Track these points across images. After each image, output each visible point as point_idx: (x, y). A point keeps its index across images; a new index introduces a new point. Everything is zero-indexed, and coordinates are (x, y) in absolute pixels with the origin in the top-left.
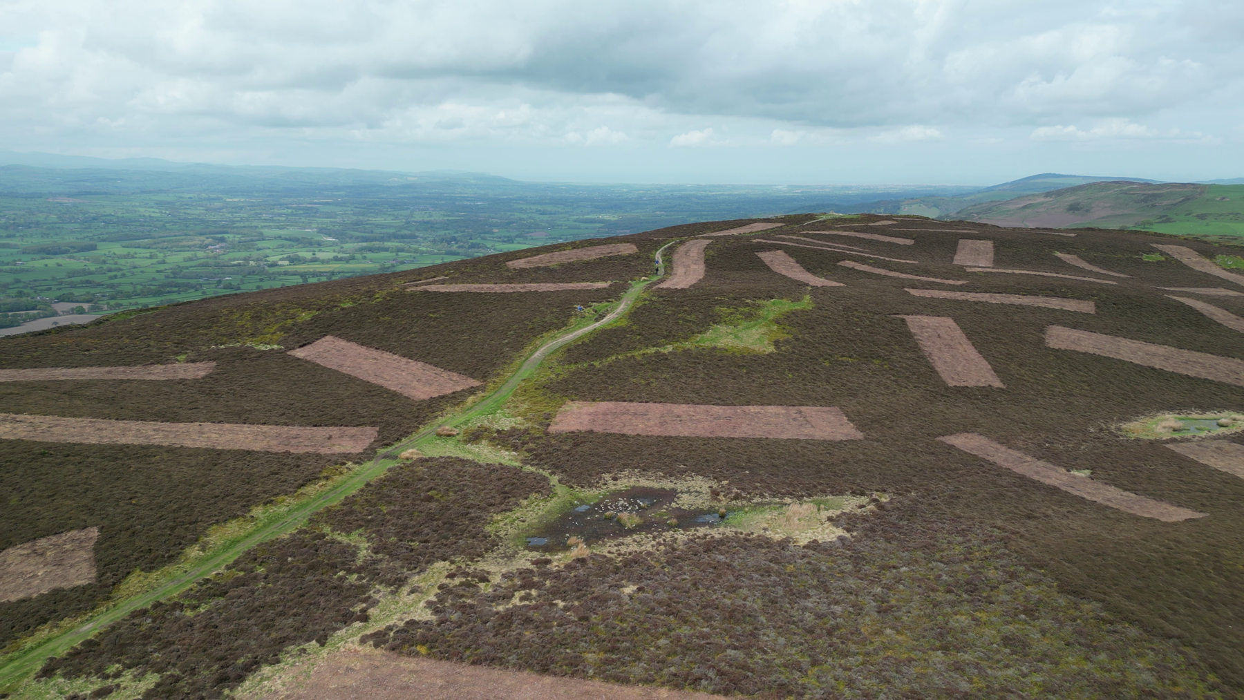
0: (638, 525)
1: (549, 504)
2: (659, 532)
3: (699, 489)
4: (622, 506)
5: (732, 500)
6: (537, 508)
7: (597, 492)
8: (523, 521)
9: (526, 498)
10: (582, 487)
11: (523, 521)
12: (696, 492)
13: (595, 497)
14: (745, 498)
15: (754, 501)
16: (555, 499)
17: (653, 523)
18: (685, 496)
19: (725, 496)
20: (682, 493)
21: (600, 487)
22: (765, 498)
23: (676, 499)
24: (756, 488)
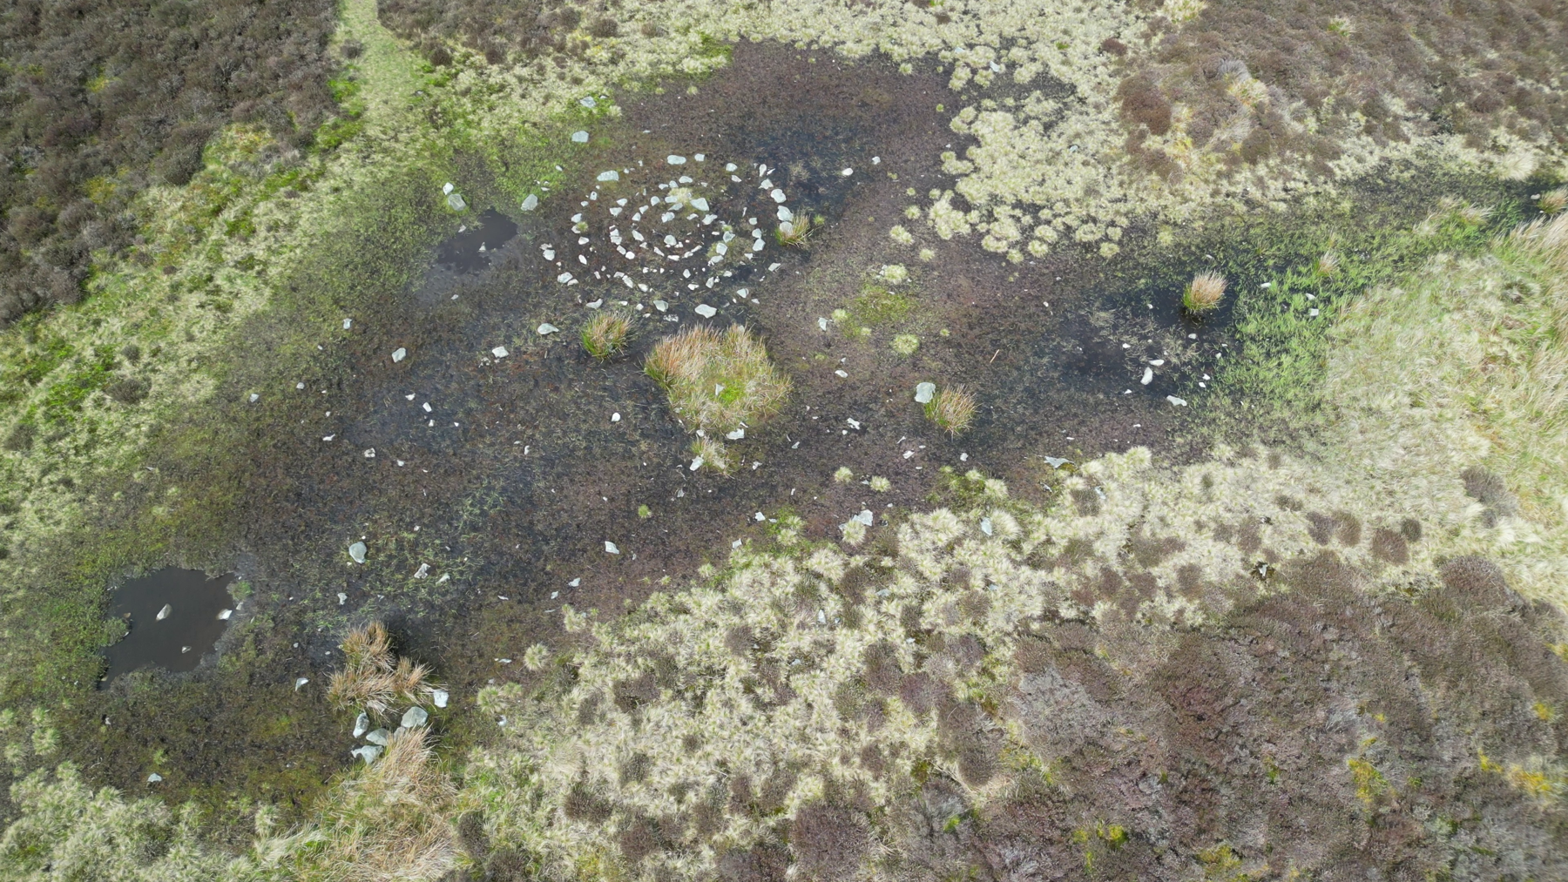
0: (764, 438)
1: (304, 206)
2: (876, 502)
3: (1057, 70)
4: (680, 226)
5: (1233, 161)
6: (234, 251)
7: (566, 92)
8: (131, 394)
9: (181, 178)
10: (495, 56)
11: (131, 394)
12: (1047, 84)
13: (550, 138)
14: (1298, 142)
15: (1346, 167)
16: (345, 166)
17: (841, 398)
18: (993, 125)
19: (1199, 136)
20: (976, 94)
21: (578, 52)
22: (1399, 136)
23: (951, 164)
24: (1337, 55)
